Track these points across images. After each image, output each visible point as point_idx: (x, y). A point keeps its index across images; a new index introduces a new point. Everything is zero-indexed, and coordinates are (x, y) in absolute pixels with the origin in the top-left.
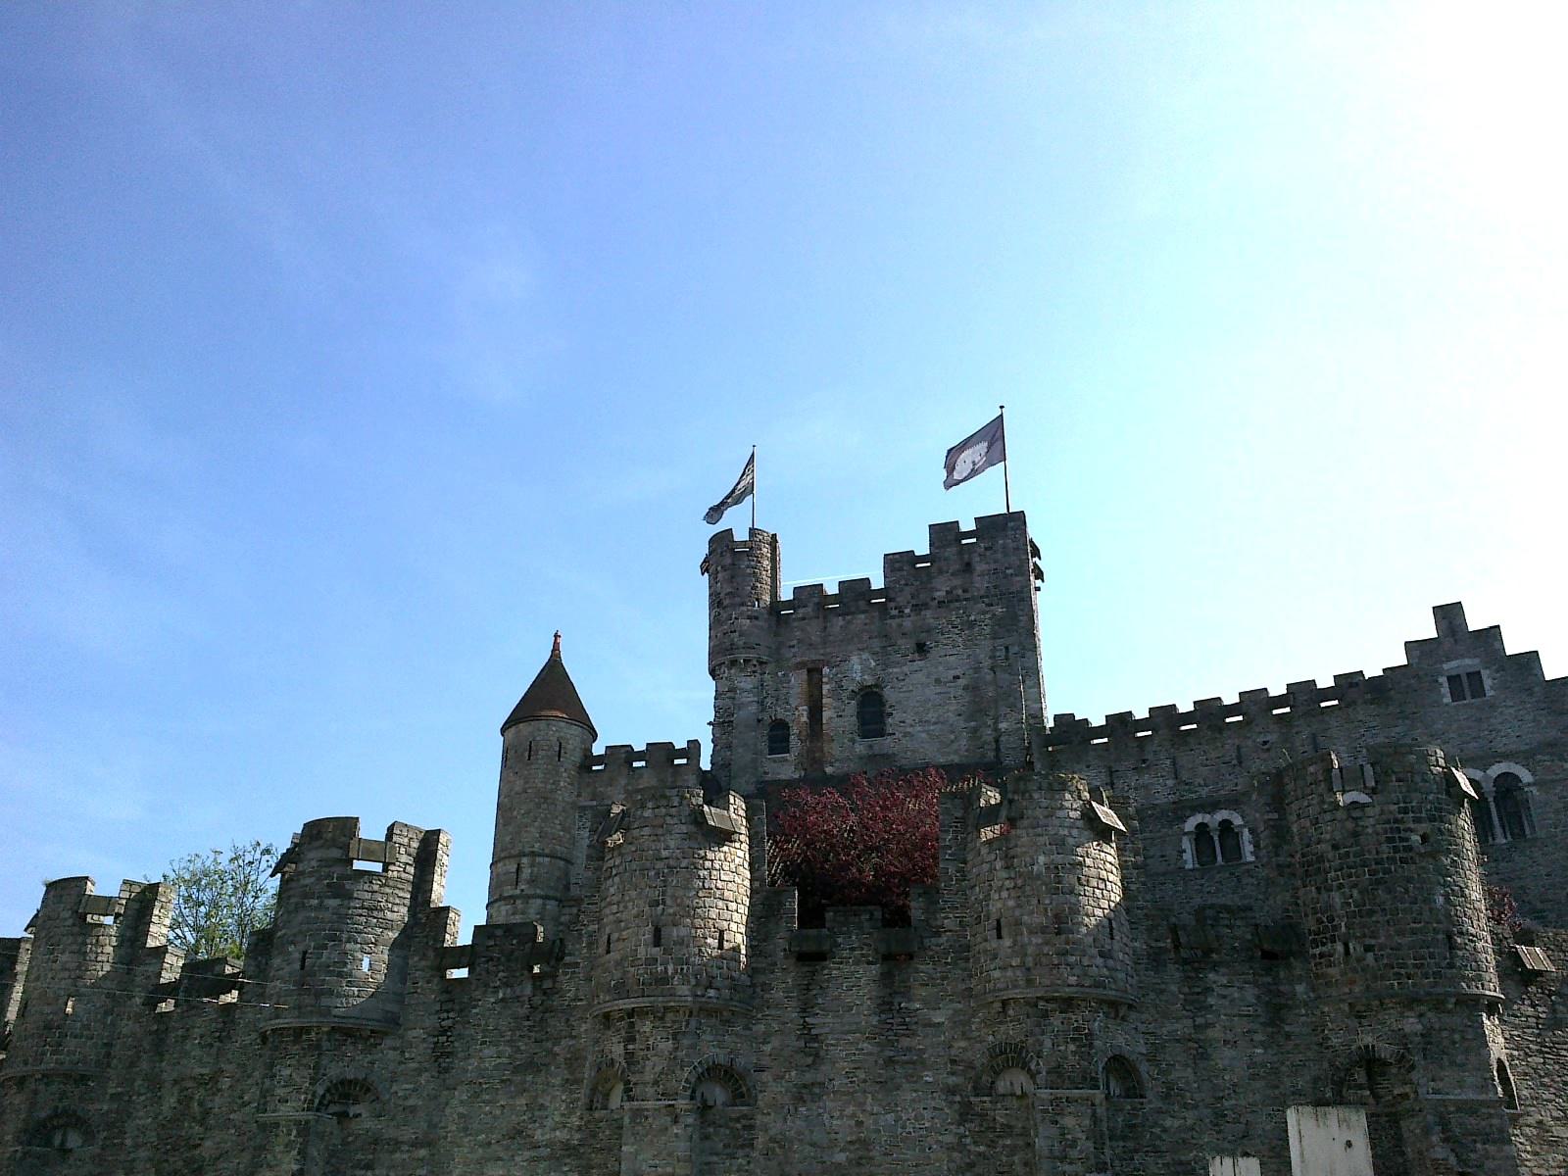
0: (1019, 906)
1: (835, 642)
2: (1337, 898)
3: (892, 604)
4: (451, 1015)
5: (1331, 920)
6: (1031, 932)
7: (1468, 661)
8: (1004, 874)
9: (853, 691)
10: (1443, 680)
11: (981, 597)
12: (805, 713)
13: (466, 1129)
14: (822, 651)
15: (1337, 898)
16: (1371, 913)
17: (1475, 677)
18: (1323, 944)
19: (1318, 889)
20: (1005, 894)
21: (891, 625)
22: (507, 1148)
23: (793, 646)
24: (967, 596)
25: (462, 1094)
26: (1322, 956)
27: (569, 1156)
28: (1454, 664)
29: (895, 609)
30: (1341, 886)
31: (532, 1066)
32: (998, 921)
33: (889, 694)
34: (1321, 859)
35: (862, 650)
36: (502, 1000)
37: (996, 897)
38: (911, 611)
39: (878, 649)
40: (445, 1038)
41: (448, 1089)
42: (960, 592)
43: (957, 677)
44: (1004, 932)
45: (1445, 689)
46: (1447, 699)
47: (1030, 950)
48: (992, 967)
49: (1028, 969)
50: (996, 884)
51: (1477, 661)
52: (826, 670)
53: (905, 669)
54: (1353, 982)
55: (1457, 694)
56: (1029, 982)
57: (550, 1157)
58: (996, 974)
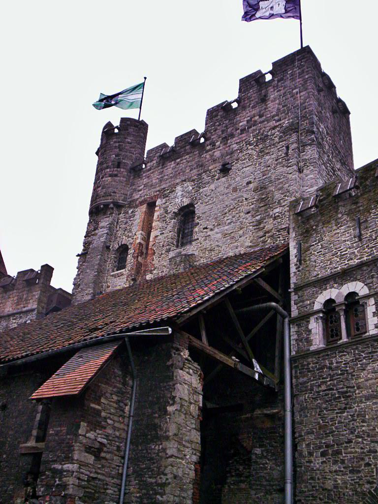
1: (167, 179)
3: (208, 142)
9: (174, 212)
11: (273, 117)
12: (139, 236)
14: (158, 189)
21: (206, 158)
23: (141, 190)
24: (262, 119)
29: (210, 145)
33: (199, 209)
35: (185, 181)
38: (221, 143)
39: (195, 177)
42: (257, 118)
43: (249, 183)
52: (159, 202)
53: (212, 187)
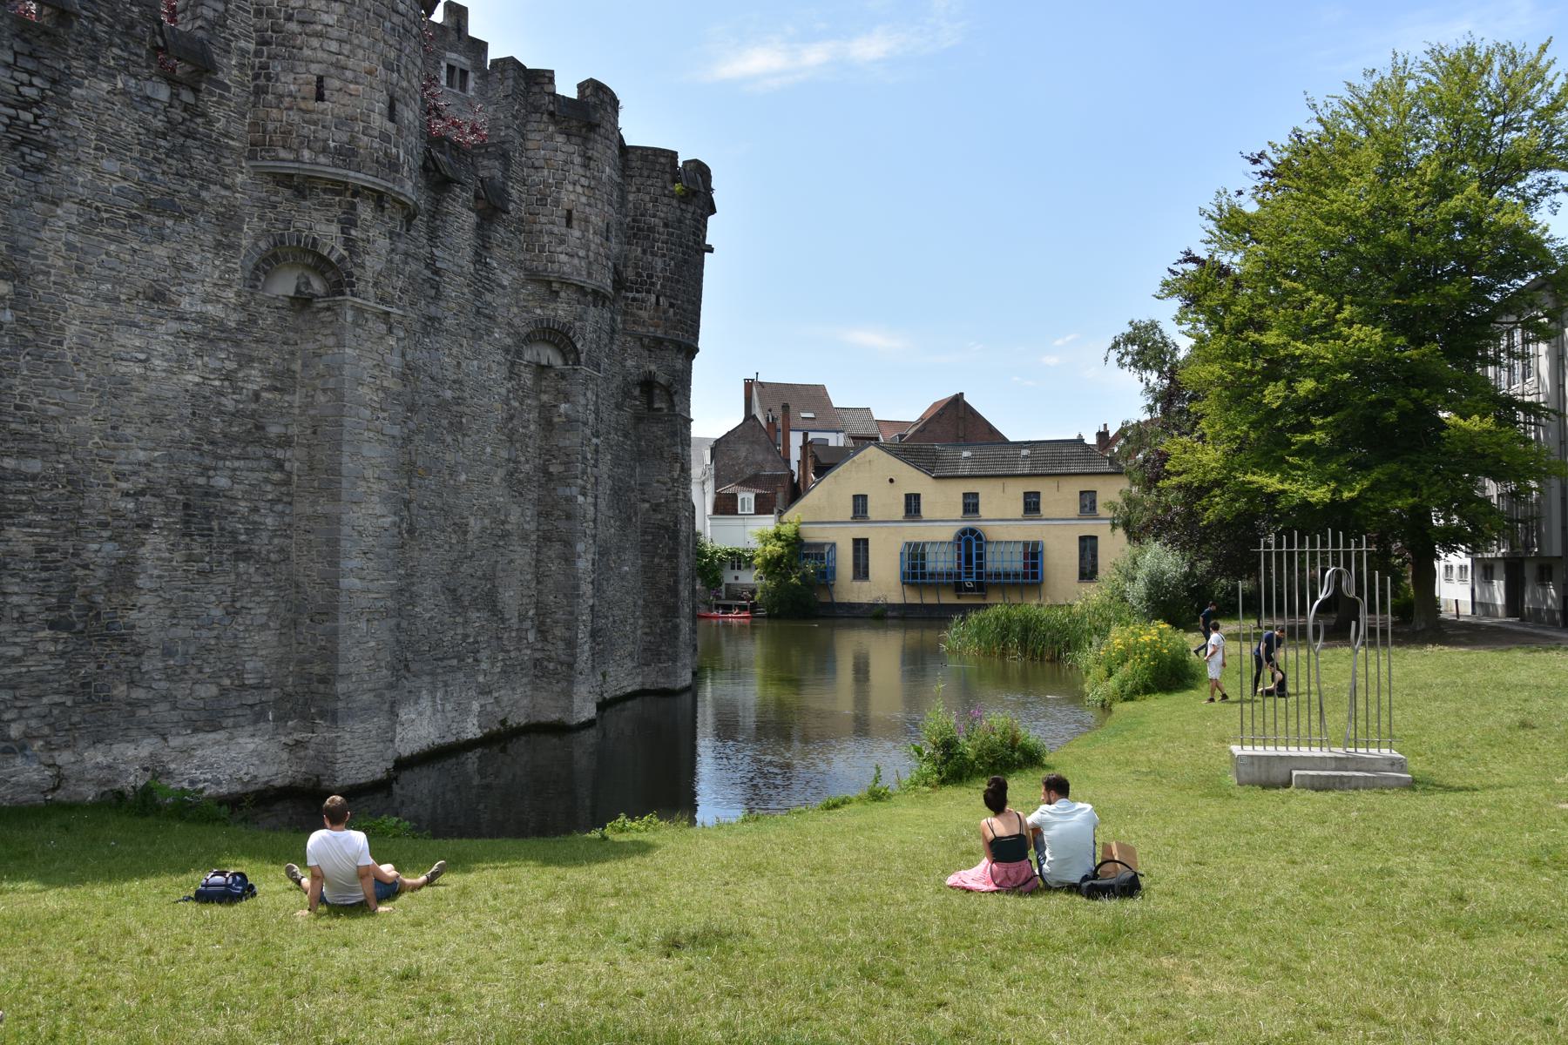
0: (589, 205)
2: (659, 263)
4: (36, 81)
5: (650, 276)
6: (595, 233)
7: (462, 59)
8: (581, 171)
10: (444, 64)
13: (79, 269)
15: (659, 263)
16: (678, 281)
17: (464, 73)
18: (638, 292)
19: (644, 252)
20: (579, 189)
22: (142, 311)
25: (67, 213)
26: (634, 299)
27: (225, 340)
28: (454, 56)
30: (664, 255)
31: (166, 206)
32: (569, 212)
34: (651, 229)
36: (124, 92)
37: (570, 188)
40: (29, 117)
41: (43, 200)
44: (575, 223)
45: (444, 73)
46: (443, 82)
47: (593, 246)
48: (559, 249)
49: (590, 263)
50: (572, 177)
51: (468, 62)
54: (657, 326)
55: (450, 83)
56: (589, 275)
57: (201, 337)
58: (563, 258)
